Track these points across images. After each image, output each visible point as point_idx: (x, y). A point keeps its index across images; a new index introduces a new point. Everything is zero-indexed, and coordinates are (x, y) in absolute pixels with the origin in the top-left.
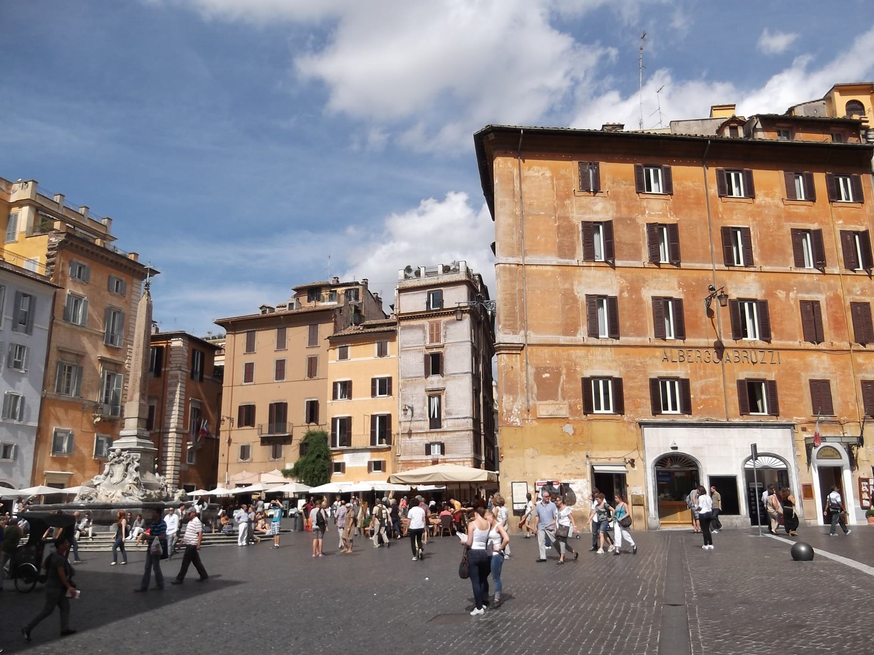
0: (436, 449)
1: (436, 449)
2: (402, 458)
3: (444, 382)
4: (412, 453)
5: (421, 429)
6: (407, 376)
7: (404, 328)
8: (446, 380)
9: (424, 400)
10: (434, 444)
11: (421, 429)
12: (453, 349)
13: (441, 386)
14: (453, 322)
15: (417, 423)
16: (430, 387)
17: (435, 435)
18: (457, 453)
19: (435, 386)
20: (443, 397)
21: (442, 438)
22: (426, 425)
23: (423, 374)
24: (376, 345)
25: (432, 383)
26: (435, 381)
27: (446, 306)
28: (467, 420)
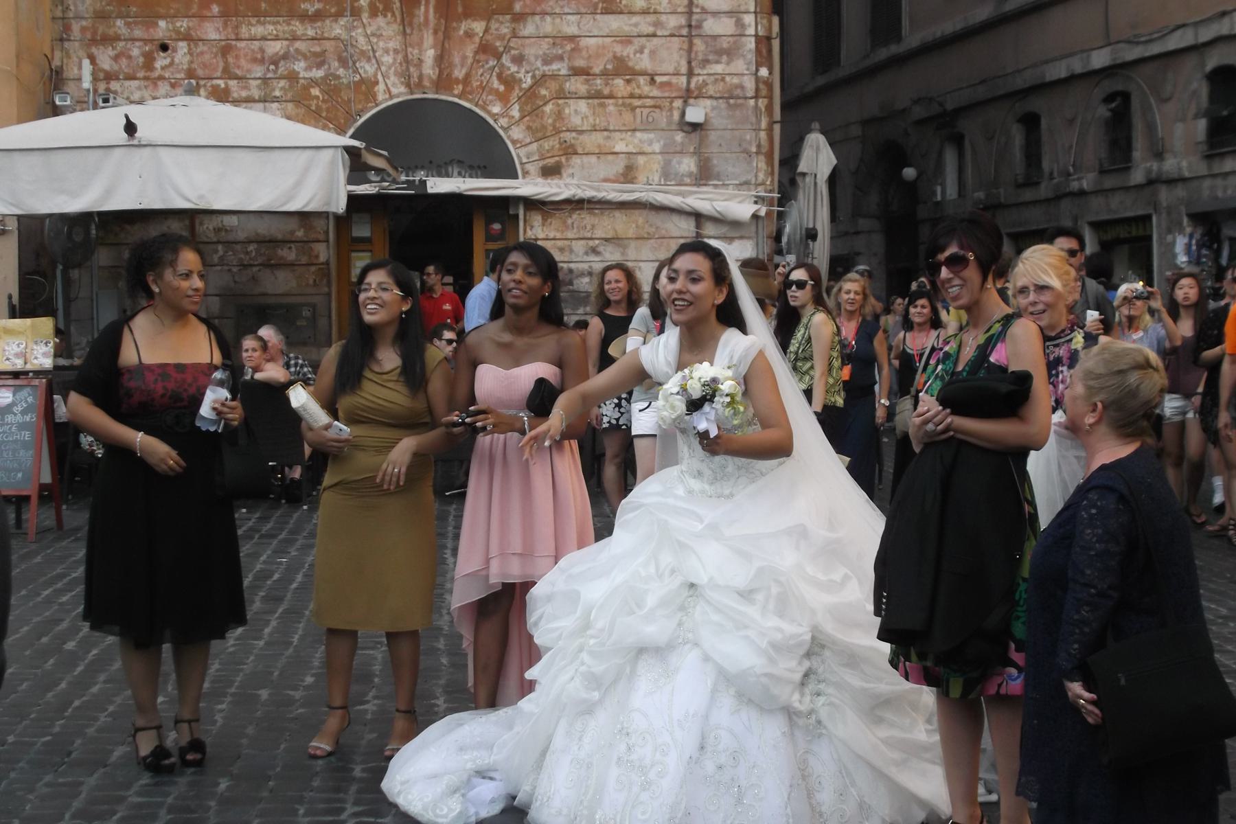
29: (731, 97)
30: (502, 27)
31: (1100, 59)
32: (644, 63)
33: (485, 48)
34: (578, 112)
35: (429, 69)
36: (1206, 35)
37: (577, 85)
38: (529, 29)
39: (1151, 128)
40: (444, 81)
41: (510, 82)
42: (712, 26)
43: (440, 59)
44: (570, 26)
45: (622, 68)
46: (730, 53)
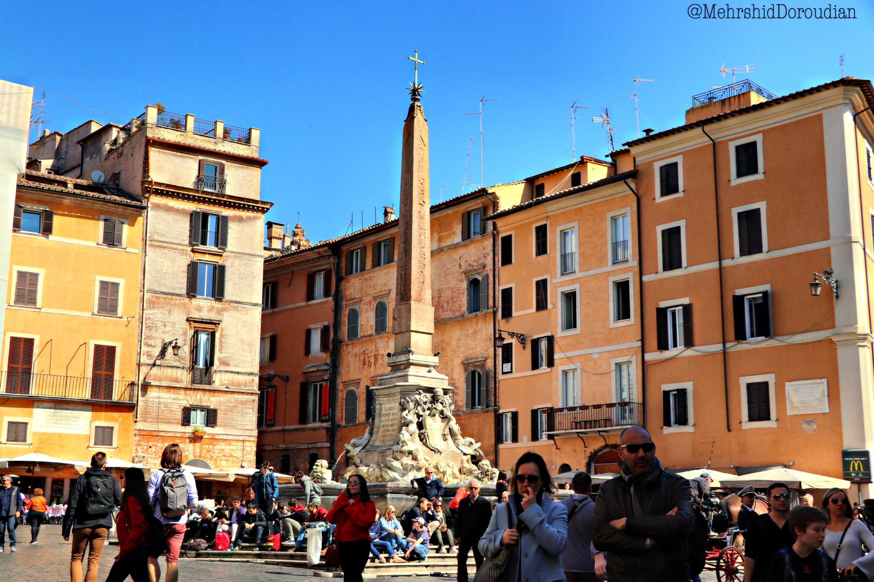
0: (198, 418)
1: (198, 418)
2: (140, 426)
3: (220, 311)
4: (159, 420)
5: (177, 381)
6: (157, 289)
7: (157, 207)
8: (224, 310)
9: (185, 334)
10: (195, 408)
11: (177, 381)
12: (237, 262)
13: (213, 316)
14: (240, 219)
15: (169, 370)
16: (196, 315)
17: (200, 395)
18: (234, 427)
19: (205, 315)
20: (217, 335)
21: (212, 401)
22: (185, 377)
23: (184, 291)
24: (101, 224)
25: (199, 309)
26: (204, 306)
27: (229, 191)
28: (251, 377)
29: (249, 462)
30: (211, 447)
31: (282, 446)
32: (235, 455)
33: (208, 451)
34: (224, 463)
35: (198, 454)
36: (310, 446)
37: (223, 458)
38: (216, 447)
39: (295, 464)
40: (200, 457)
41: (212, 457)
42: (247, 449)
43: (200, 452)
44: (223, 447)
45: (231, 456)
46: (250, 454)
